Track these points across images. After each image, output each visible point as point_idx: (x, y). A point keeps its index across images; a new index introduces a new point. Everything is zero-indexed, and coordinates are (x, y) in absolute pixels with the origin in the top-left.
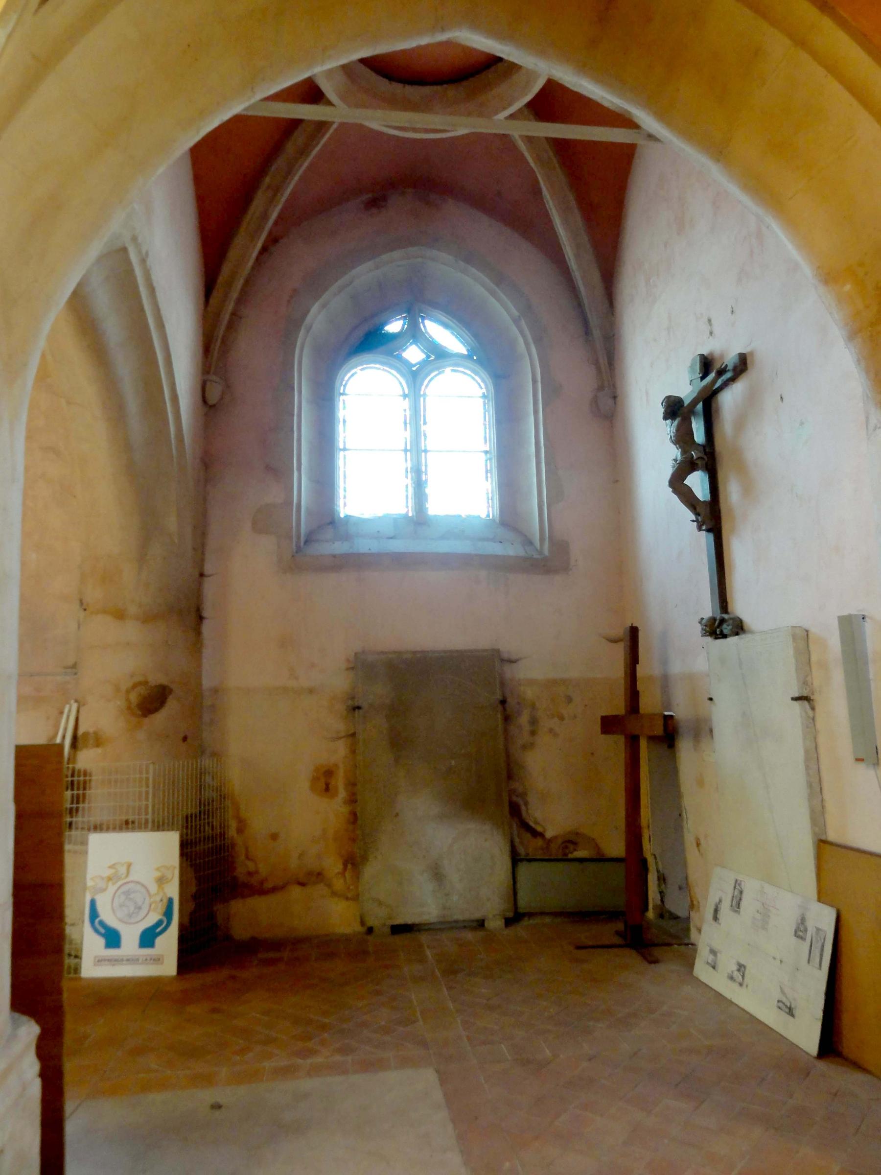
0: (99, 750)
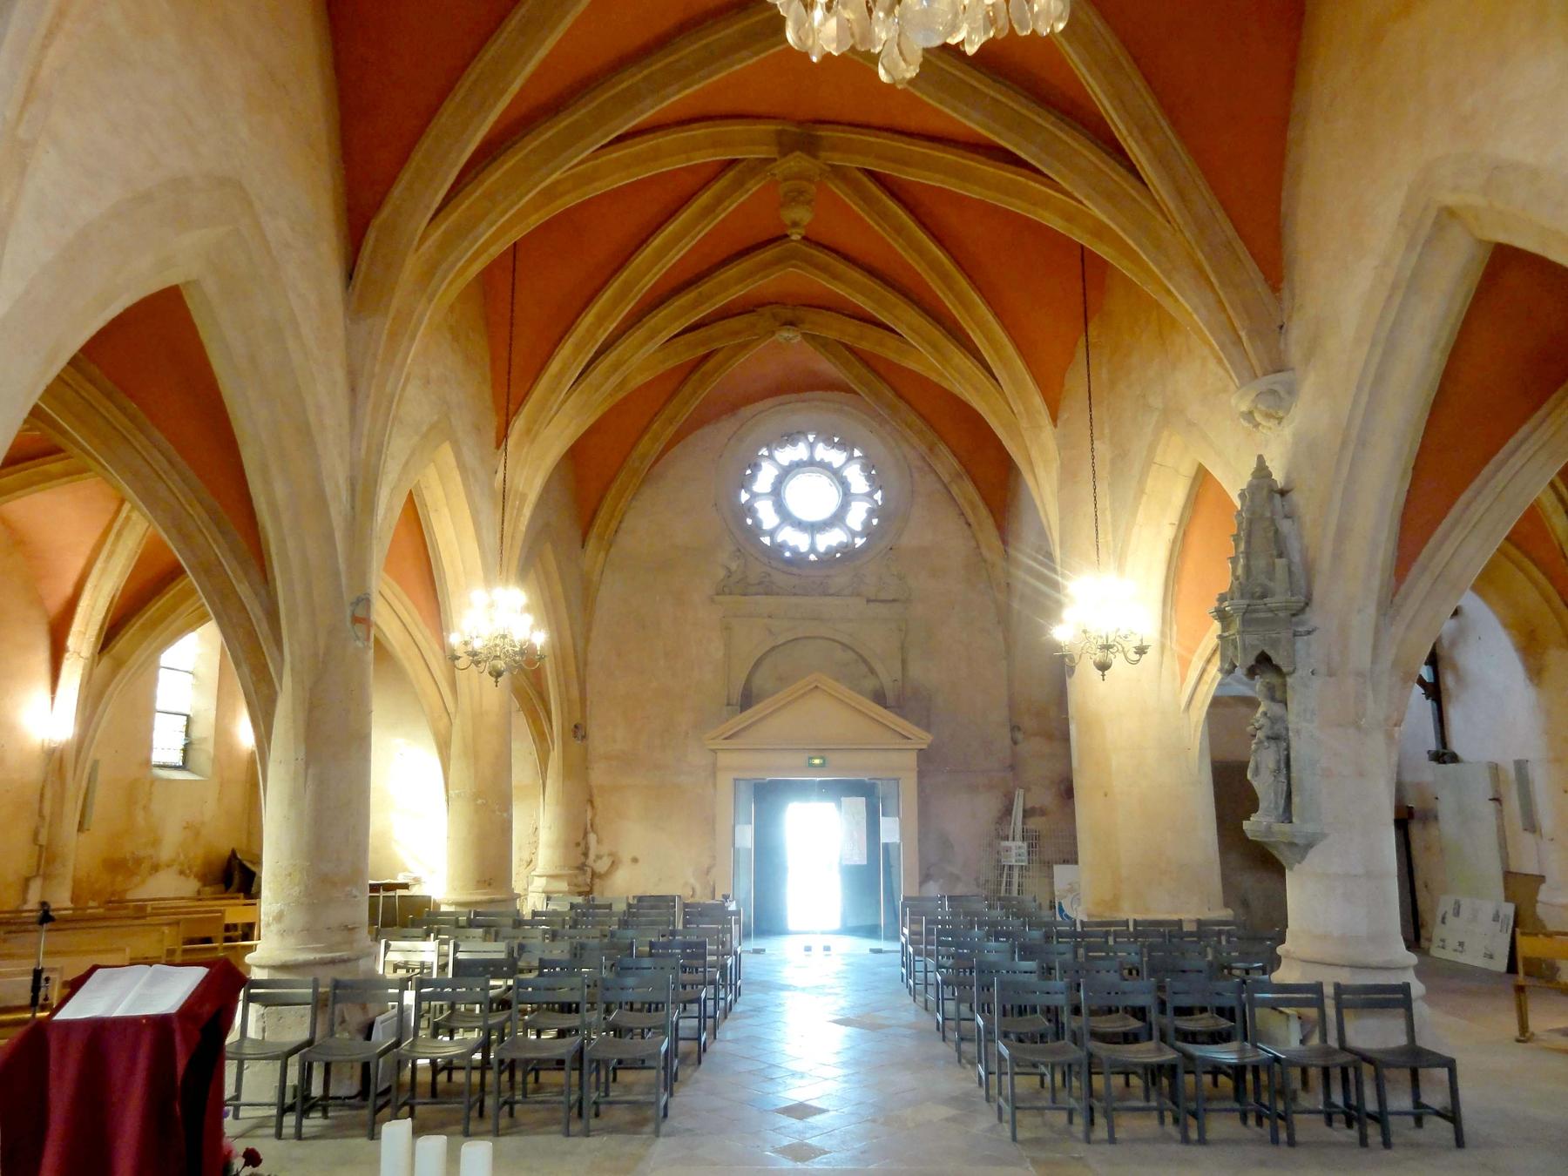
0: (1044, 818)
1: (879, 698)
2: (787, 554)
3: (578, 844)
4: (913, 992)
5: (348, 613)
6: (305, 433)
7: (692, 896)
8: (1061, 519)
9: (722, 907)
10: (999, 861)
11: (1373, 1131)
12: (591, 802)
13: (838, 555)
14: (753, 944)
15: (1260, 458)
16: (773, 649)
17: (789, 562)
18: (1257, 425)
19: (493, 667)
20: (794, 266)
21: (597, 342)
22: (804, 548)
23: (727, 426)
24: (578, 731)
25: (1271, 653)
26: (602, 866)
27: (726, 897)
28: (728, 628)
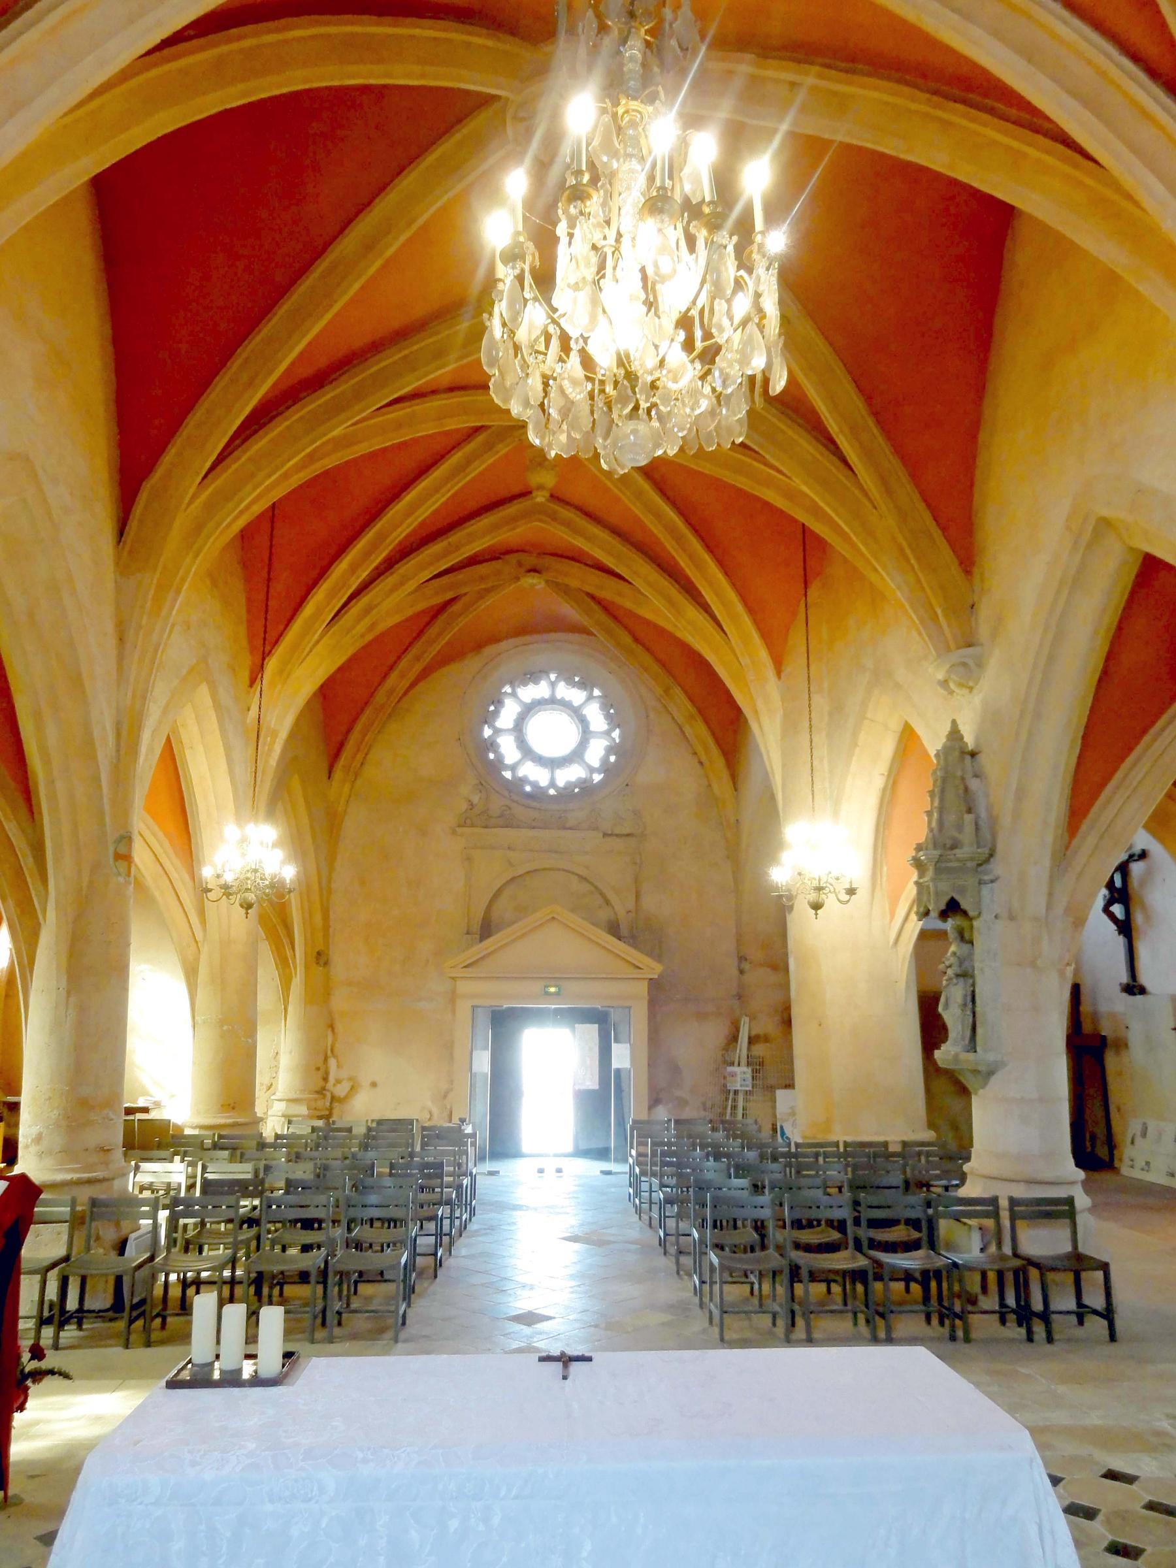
1: (614, 929)
2: (528, 789)
3: (318, 1069)
4: (639, 1211)
5: (111, 850)
6: (77, 682)
7: (430, 1119)
8: (784, 766)
9: (459, 1130)
10: (725, 1086)
11: (1039, 1329)
12: (332, 1027)
13: (577, 790)
14: (488, 1166)
15: (954, 722)
16: (513, 879)
17: (529, 796)
18: (951, 692)
19: (245, 899)
20: (540, 521)
21: (350, 587)
22: (544, 782)
23: (472, 664)
24: (321, 958)
25: (957, 898)
26: (341, 1090)
27: (463, 1121)
28: (469, 859)
